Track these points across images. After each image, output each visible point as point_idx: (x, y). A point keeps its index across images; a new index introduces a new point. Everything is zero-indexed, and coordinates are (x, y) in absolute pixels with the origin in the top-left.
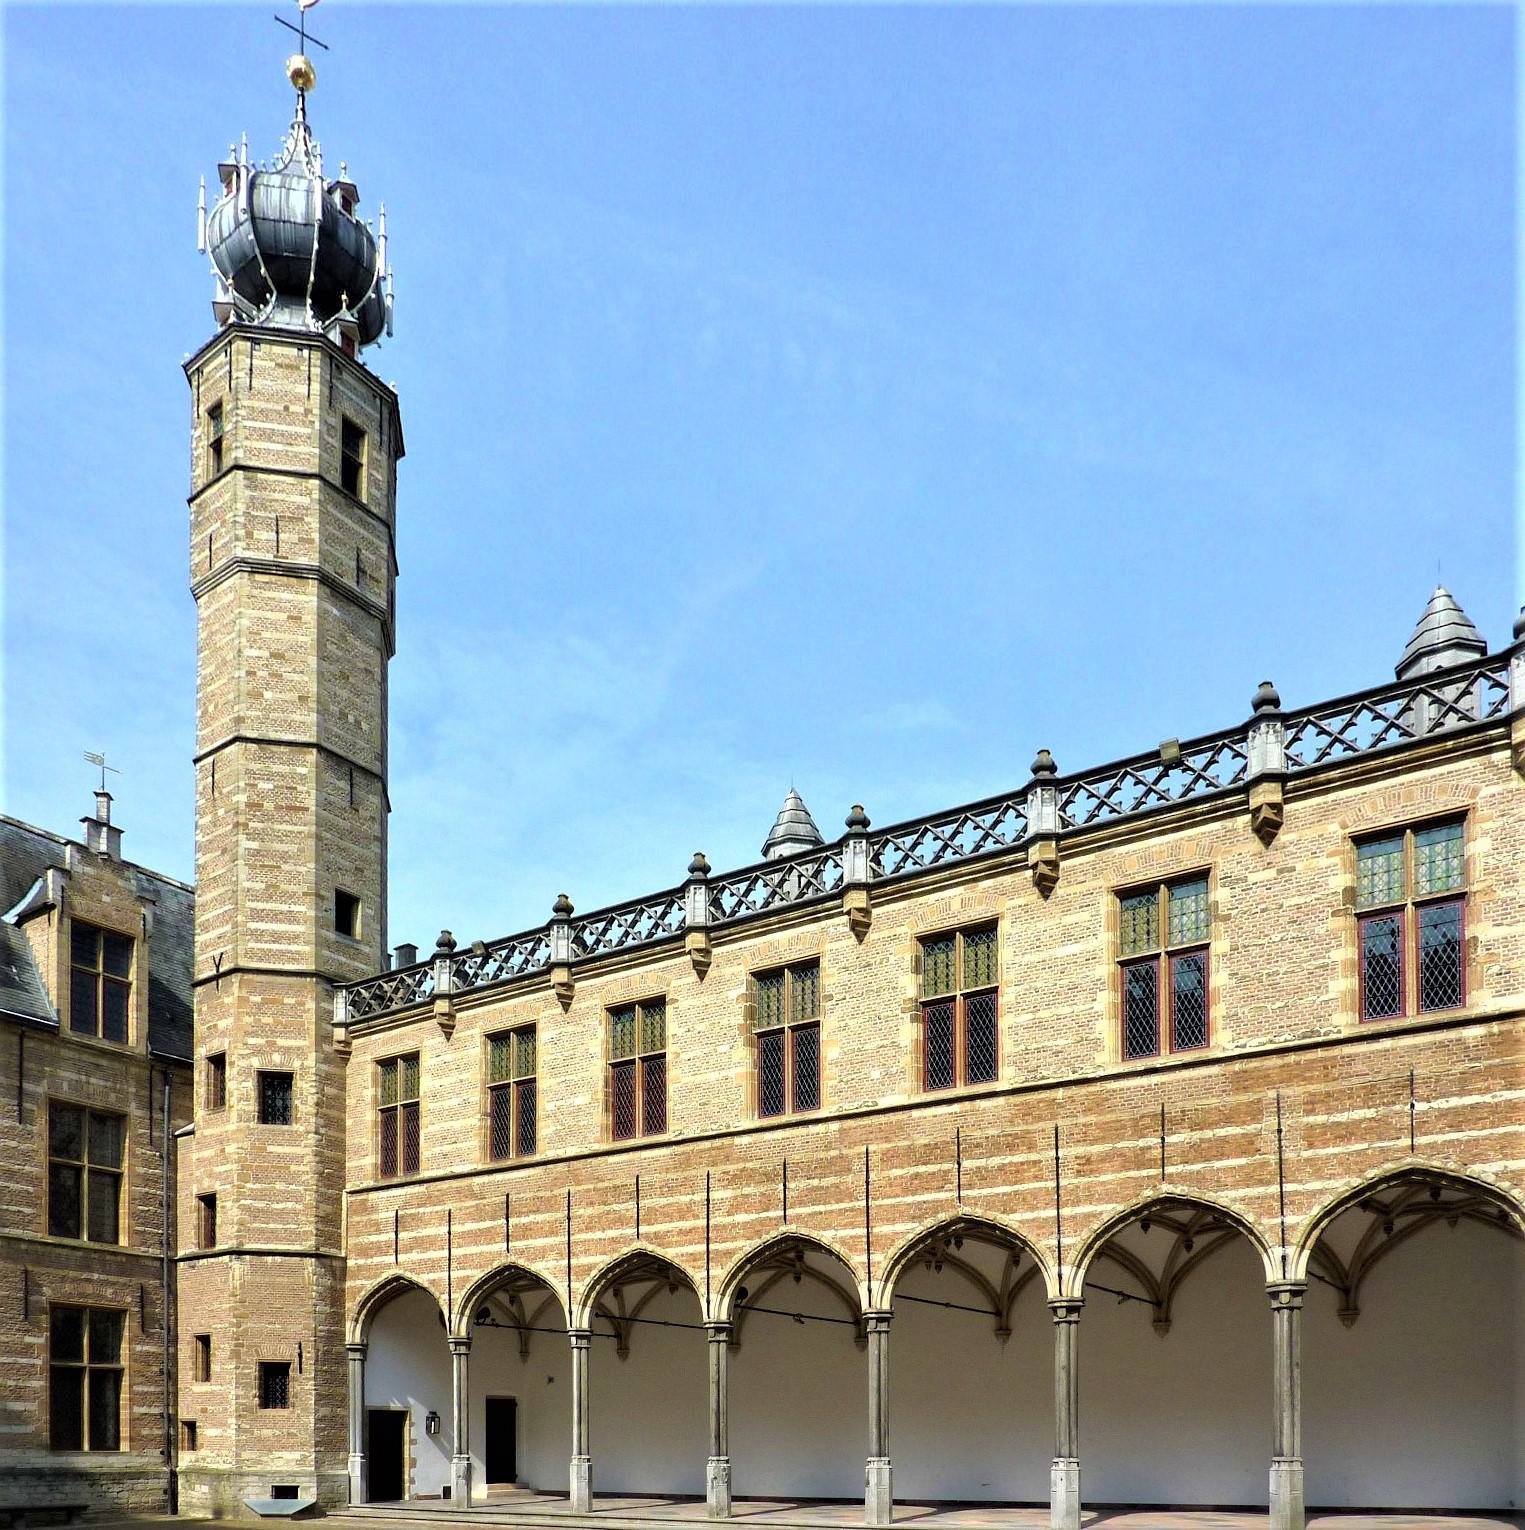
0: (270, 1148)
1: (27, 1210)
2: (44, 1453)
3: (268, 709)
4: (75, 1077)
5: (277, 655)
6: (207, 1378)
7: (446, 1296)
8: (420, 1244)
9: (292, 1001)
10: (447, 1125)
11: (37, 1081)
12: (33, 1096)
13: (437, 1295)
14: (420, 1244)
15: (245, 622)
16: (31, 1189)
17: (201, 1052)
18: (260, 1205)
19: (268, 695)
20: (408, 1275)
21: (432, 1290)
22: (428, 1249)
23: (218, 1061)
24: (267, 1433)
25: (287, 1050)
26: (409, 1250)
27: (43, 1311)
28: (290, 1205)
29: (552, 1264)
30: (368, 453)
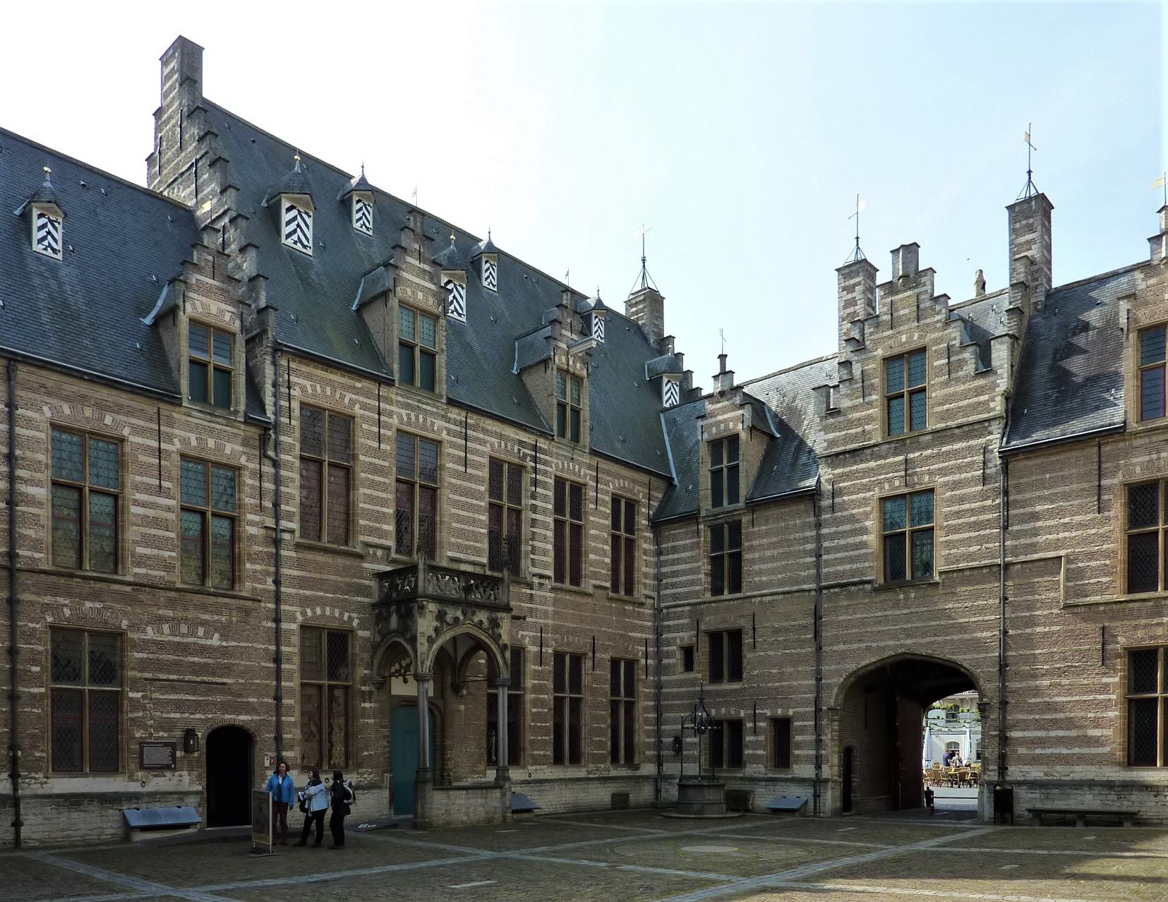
1: (1104, 580)
2: (1117, 768)
16: (1108, 562)
27: (1118, 656)
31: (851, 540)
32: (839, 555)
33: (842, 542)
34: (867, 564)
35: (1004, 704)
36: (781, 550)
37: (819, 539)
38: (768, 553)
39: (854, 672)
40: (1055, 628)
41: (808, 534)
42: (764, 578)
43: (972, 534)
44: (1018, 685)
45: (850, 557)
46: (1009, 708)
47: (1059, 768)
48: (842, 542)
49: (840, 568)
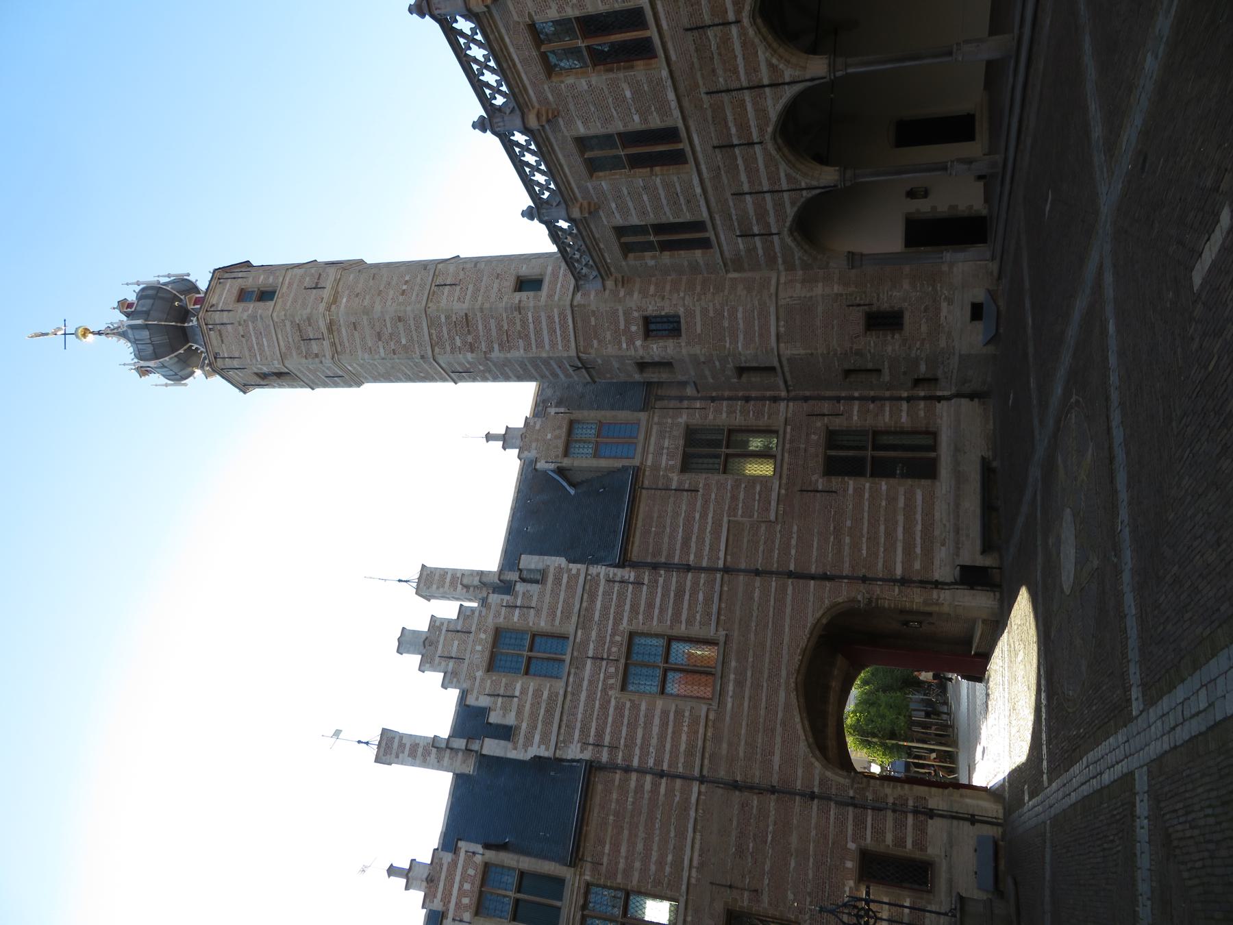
0: (699, 331)
1: (758, 488)
3: (411, 340)
4: (665, 457)
5: (379, 336)
6: (879, 371)
7: (804, 193)
8: (762, 215)
9: (593, 319)
10: (664, 202)
11: (671, 480)
12: (680, 482)
13: (803, 200)
14: (762, 215)
15: (366, 356)
17: (637, 377)
18: (741, 337)
19: (404, 342)
20: (788, 224)
21: (799, 204)
22: (766, 210)
23: (642, 366)
24: (924, 328)
25: (628, 323)
26: (768, 225)
28: (740, 315)
29: (769, 102)
30: (250, 282)
31: (655, 730)
32: (668, 747)
33: (654, 741)
34: (687, 714)
35: (864, 579)
36: (641, 828)
37: (642, 771)
38: (640, 847)
39: (809, 746)
40: (795, 528)
41: (633, 784)
42: (670, 858)
43: (687, 597)
44: (847, 565)
45: (674, 732)
46: (870, 575)
47: (937, 533)
48: (654, 741)
49: (683, 747)
